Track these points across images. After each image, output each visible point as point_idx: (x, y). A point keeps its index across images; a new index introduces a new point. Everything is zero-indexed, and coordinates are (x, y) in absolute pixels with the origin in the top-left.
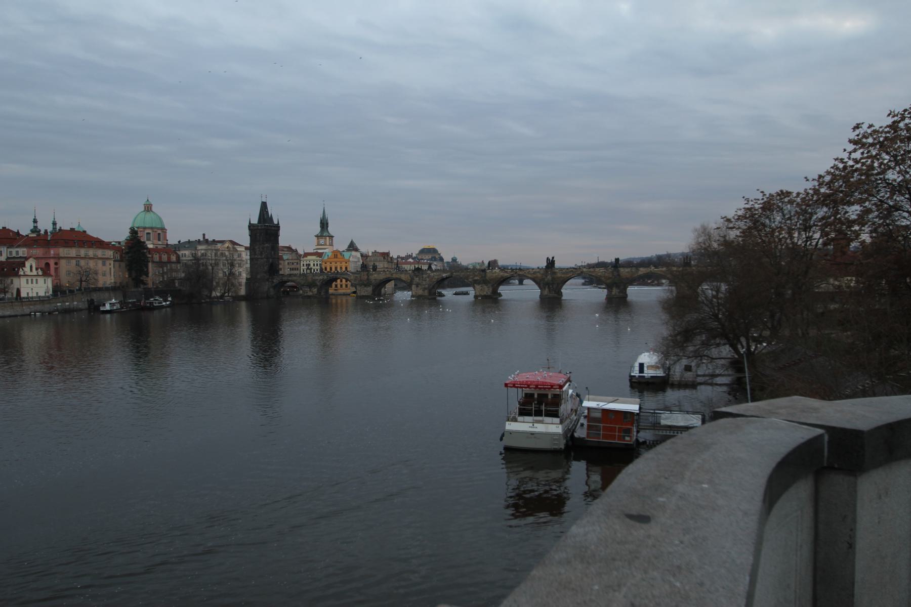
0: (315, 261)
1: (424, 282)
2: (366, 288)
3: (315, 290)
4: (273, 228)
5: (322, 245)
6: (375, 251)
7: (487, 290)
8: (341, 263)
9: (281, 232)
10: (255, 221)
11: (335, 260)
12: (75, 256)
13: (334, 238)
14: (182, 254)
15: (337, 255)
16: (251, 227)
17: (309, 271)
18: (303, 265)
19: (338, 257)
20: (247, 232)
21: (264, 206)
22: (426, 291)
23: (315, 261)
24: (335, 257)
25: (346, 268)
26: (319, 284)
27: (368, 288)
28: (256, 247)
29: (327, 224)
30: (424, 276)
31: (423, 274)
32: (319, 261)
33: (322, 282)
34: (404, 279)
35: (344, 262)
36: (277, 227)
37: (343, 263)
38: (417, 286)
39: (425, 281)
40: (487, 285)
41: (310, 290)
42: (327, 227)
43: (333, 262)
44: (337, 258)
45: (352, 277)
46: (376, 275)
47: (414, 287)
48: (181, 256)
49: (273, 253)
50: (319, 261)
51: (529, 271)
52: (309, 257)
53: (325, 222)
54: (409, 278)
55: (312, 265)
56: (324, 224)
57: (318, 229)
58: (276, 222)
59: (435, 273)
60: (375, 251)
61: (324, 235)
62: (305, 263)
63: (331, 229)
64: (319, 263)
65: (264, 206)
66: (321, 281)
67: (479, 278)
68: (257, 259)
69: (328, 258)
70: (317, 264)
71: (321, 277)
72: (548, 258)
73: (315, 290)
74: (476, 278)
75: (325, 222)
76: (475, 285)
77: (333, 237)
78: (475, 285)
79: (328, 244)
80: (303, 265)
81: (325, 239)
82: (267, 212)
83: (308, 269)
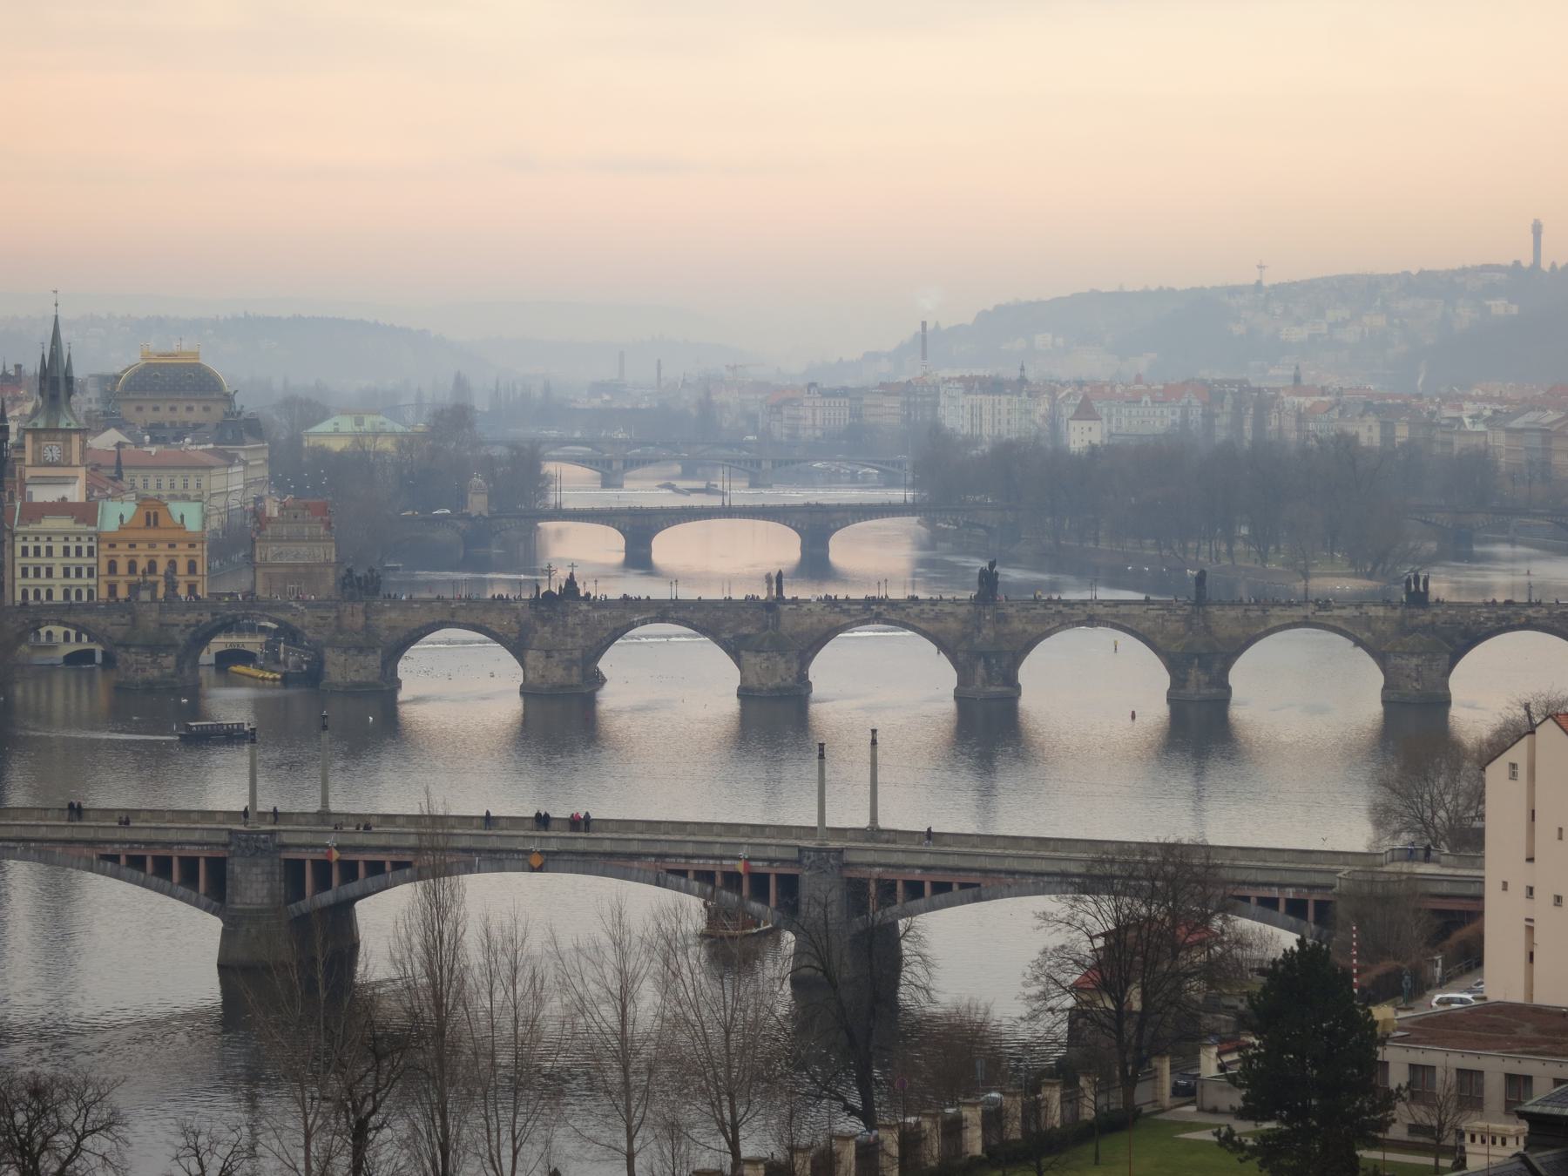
1: (569, 640)
2: (361, 658)
3: (169, 661)
7: (780, 672)
8: (152, 546)
11: (152, 534)
15: (156, 515)
18: (25, 551)
19: (161, 523)
22: (575, 670)
24: (148, 523)
26: (181, 639)
27: (370, 657)
30: (570, 620)
31: (565, 615)
32: (85, 539)
34: (496, 629)
35: (182, 541)
37: (159, 546)
38: (549, 656)
39: (573, 636)
40: (783, 655)
41: (154, 662)
43: (141, 541)
44: (156, 523)
45: (307, 619)
46: (393, 615)
47: (531, 656)
51: (922, 611)
52: (50, 524)
53: (62, 376)
54: (516, 627)
55: (58, 550)
59: (607, 613)
61: (62, 425)
66: (192, 629)
67: (753, 631)
69: (122, 527)
70: (79, 551)
71: (191, 617)
73: (169, 661)
74: (745, 630)
75: (62, 376)
76: (743, 653)
78: (743, 653)
80: (25, 551)
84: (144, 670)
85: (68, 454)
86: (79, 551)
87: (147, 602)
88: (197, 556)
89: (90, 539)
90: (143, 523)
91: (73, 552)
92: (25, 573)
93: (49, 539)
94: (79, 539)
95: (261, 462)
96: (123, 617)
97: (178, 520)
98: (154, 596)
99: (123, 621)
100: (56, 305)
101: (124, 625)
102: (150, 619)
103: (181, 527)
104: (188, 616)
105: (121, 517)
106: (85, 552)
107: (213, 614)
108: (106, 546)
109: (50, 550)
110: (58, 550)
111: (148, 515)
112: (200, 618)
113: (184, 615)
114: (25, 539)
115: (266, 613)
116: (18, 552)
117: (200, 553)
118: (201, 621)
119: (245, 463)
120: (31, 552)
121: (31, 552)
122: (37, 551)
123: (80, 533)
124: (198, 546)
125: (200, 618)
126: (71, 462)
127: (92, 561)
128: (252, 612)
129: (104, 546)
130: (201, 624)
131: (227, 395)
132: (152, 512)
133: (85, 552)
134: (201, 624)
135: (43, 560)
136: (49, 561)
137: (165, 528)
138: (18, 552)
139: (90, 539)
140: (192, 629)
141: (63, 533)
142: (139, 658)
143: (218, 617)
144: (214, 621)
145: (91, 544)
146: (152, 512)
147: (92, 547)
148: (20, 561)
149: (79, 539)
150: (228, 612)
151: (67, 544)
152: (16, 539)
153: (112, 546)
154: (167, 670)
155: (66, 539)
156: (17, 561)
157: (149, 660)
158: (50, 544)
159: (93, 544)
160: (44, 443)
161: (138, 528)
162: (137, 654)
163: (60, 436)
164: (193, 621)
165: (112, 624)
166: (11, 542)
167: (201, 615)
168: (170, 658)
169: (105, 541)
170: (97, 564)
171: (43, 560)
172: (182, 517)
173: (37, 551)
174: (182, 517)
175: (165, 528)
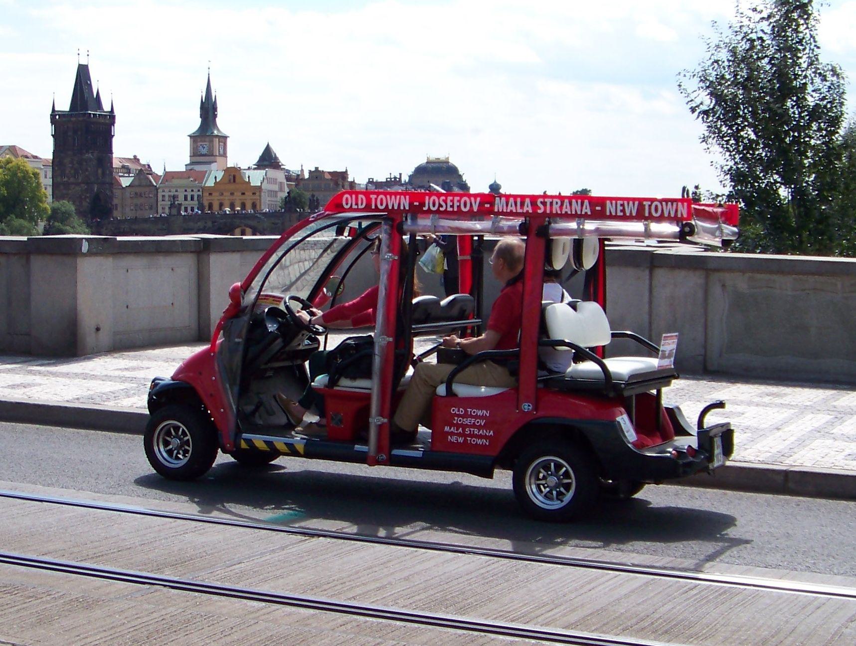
0: (189, 190)
6: (317, 168)
9: (118, 130)
10: (64, 105)
11: (232, 187)
16: (57, 118)
17: (174, 211)
18: (163, 196)
19: (237, 180)
20: (48, 129)
21: (83, 74)
23: (189, 190)
25: (254, 206)
28: (67, 161)
29: (215, 109)
42: (215, 116)
44: (234, 181)
49: (100, 171)
52: (176, 182)
53: (210, 106)
55: (181, 199)
56: (208, 109)
57: (195, 122)
58: (107, 108)
60: (317, 168)
62: (167, 194)
63: (223, 123)
64: (196, 194)
65: (83, 74)
68: (67, 185)
72: (684, 189)
75: (210, 106)
77: (226, 137)
81: (212, 141)
82: (90, 85)
83: (172, 206)
87: (175, 215)
89: (199, 191)
93: (176, 191)
94: (192, 191)
105: (216, 178)
107: (213, 222)
114: (163, 191)
116: (160, 198)
124: (258, 194)
139: (199, 191)
151: (186, 193)
152: (159, 191)
153: (210, 194)
155: (186, 191)
163: (207, 139)
164: (201, 227)
172: (249, 177)
174: (249, 177)
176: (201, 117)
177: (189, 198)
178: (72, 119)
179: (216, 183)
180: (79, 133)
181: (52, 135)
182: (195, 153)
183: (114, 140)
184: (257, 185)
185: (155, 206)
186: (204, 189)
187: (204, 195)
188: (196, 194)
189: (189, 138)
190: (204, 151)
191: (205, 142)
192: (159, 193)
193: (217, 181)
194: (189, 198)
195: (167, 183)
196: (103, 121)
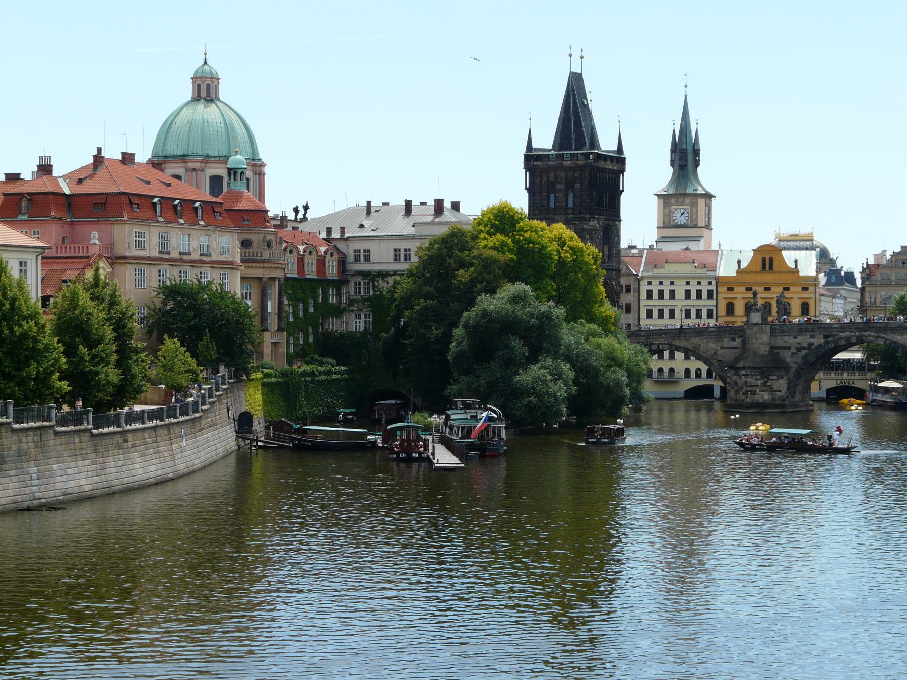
0: (693, 282)
3: (781, 385)
4: (609, 166)
5: (678, 226)
10: (545, 141)
11: (767, 277)
12: (157, 255)
13: (714, 203)
14: (357, 251)
15: (771, 260)
17: (756, 318)
18: (650, 294)
19: (775, 268)
23: (693, 282)
24: (764, 268)
25: (805, 309)
29: (696, 153)
32: (705, 282)
33: (804, 357)
36: (618, 160)
41: (764, 385)
42: (697, 163)
44: (771, 268)
48: (351, 259)
50: (705, 282)
53: (690, 149)
55: (680, 294)
58: (607, 144)
61: (690, 191)
62: (655, 289)
64: (705, 289)
66: (804, 352)
70: (699, 294)
71: (804, 340)
73: (781, 385)
75: (690, 149)
77: (709, 197)
79: (702, 222)
80: (650, 294)
81: (694, 205)
84: (754, 393)
85: (694, 216)
86: (699, 294)
87: (758, 324)
88: (810, 298)
89: (710, 283)
90: (760, 267)
91: (694, 295)
92: (649, 314)
93: (672, 283)
94: (699, 283)
95: (856, 301)
96: (733, 340)
97: (792, 266)
98: (764, 320)
99: (734, 344)
100: (686, 86)
101: (734, 348)
102: (760, 341)
103: (795, 271)
104: (800, 339)
105: (739, 262)
106: (705, 295)
107: (825, 337)
108: (725, 289)
109: (672, 294)
110: (680, 294)
111: (764, 260)
112: (812, 340)
113: (795, 338)
114: (650, 283)
115: (880, 335)
116: (644, 295)
117: (812, 295)
118: (813, 344)
119: (845, 298)
120: (655, 295)
121: (655, 295)
122: (661, 294)
123: (700, 277)
124: (811, 289)
125: (812, 340)
126: (697, 225)
127: (712, 303)
128: (867, 334)
129: (723, 289)
130: (813, 347)
131: (832, 260)
132: (767, 257)
133: (705, 295)
134: (813, 347)
135: (666, 303)
136: (672, 302)
137: (779, 272)
138: (644, 295)
139: (710, 283)
140: (804, 352)
141: (685, 277)
142: (749, 380)
143: (832, 339)
144: (827, 343)
145: (710, 287)
146: (767, 257)
147: (712, 290)
148: (645, 303)
149: (699, 283)
150: (842, 335)
151: (688, 287)
152: (642, 283)
153: (730, 289)
154: (778, 394)
155: (688, 283)
156: (642, 303)
157: (759, 382)
158: (672, 287)
159: (713, 287)
160: (674, 207)
161: (756, 272)
162: (746, 376)
163: (687, 201)
164: (806, 345)
165: (722, 348)
166: (637, 286)
167: (813, 337)
168: (781, 381)
169: (723, 285)
170: (716, 306)
171: (666, 303)
172: (796, 262)
173: (661, 294)
175: (779, 272)
176: (672, 165)
177: (666, 295)
178: (564, 162)
179: (739, 271)
180: (577, 186)
181: (526, 189)
182: (666, 223)
183: (623, 198)
184: (809, 274)
185: (634, 307)
186: (718, 279)
187: (720, 289)
188: (705, 289)
189: (656, 198)
190: (682, 220)
191: (682, 204)
192: (642, 287)
193: (742, 267)
194: (666, 295)
195: (655, 271)
196: (610, 167)
